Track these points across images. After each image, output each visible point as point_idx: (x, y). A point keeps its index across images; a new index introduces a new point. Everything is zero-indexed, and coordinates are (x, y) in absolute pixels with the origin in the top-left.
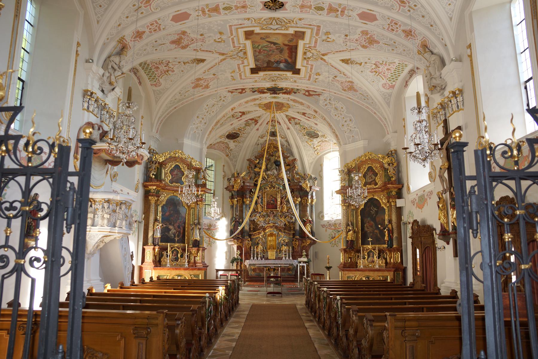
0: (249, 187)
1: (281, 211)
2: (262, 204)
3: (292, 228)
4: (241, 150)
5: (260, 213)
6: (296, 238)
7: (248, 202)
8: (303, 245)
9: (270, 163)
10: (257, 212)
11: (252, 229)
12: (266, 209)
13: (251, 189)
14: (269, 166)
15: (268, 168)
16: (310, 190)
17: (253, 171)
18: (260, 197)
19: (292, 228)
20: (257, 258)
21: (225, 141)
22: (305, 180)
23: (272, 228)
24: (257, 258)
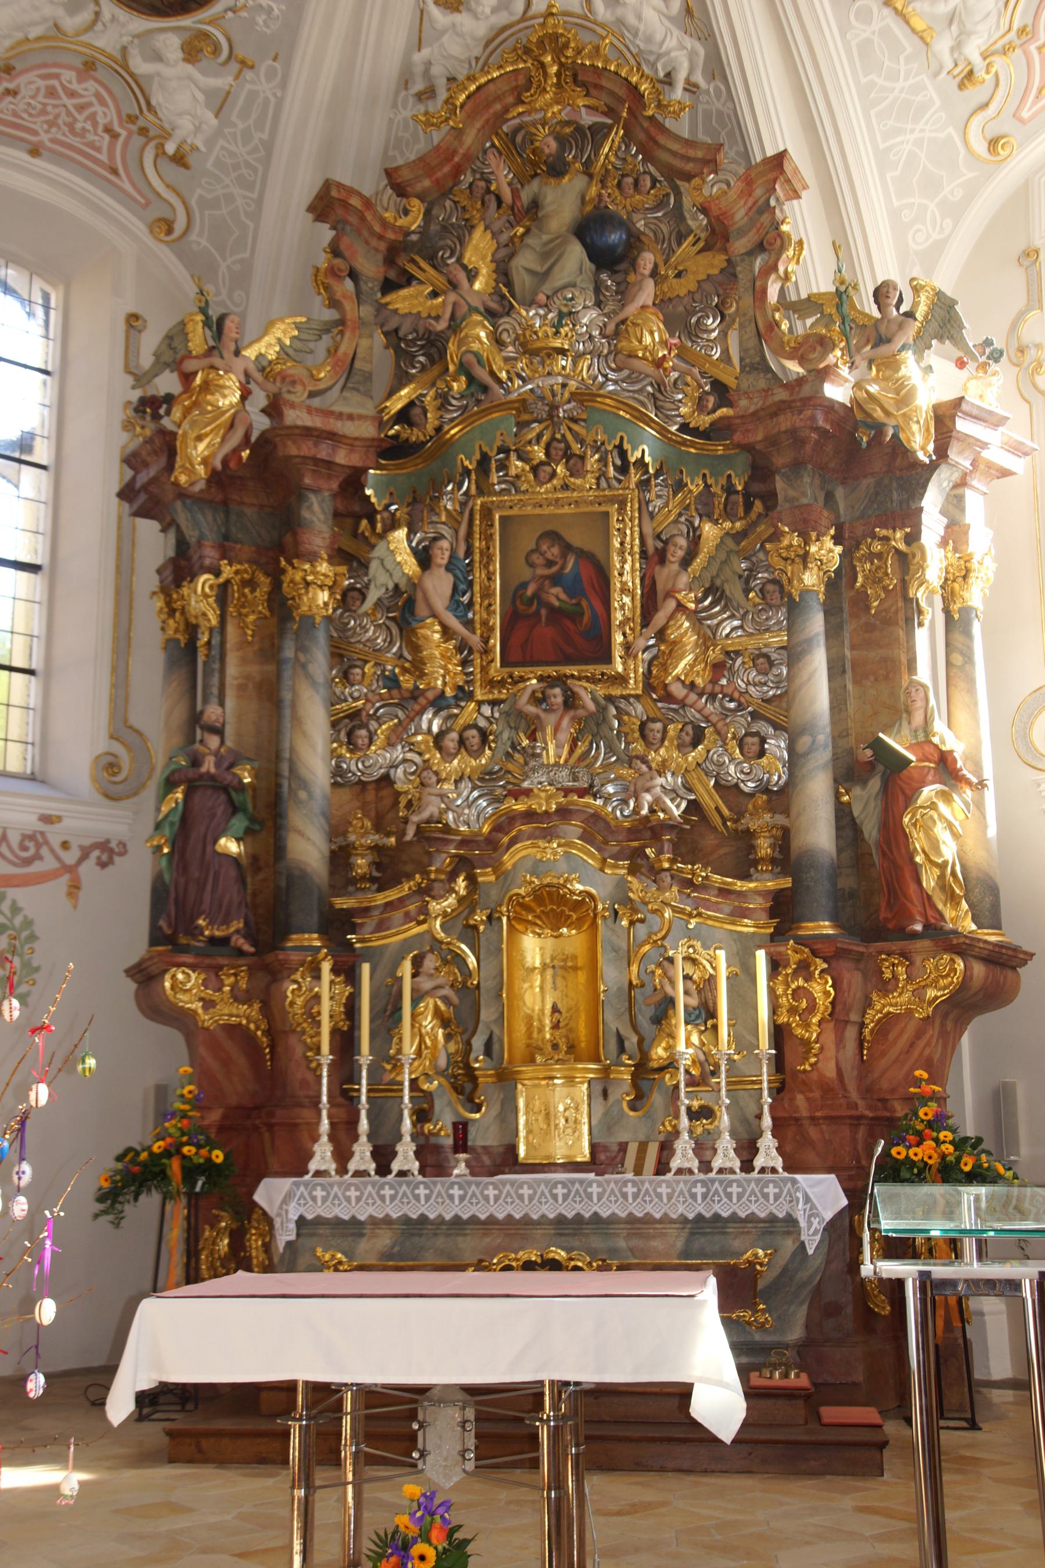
0: (323, 452)
1: (649, 686)
2: (469, 624)
3: (764, 846)
4: (269, 147)
5: (439, 703)
6: (801, 941)
7: (323, 596)
8: (883, 1006)
9: (530, 241)
10: (415, 694)
11: (361, 864)
12: (496, 669)
13: (354, 482)
14: (525, 261)
15: (521, 279)
16: (942, 452)
17: (367, 311)
18: (442, 554)
19: (764, 846)
20: (383, 1157)
21: (106, 41)
22: (889, 341)
23: (548, 835)
24: (383, 1157)
